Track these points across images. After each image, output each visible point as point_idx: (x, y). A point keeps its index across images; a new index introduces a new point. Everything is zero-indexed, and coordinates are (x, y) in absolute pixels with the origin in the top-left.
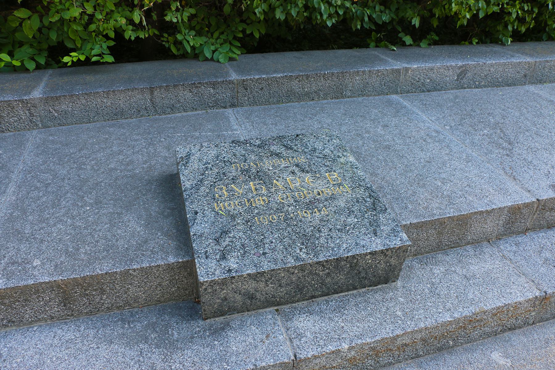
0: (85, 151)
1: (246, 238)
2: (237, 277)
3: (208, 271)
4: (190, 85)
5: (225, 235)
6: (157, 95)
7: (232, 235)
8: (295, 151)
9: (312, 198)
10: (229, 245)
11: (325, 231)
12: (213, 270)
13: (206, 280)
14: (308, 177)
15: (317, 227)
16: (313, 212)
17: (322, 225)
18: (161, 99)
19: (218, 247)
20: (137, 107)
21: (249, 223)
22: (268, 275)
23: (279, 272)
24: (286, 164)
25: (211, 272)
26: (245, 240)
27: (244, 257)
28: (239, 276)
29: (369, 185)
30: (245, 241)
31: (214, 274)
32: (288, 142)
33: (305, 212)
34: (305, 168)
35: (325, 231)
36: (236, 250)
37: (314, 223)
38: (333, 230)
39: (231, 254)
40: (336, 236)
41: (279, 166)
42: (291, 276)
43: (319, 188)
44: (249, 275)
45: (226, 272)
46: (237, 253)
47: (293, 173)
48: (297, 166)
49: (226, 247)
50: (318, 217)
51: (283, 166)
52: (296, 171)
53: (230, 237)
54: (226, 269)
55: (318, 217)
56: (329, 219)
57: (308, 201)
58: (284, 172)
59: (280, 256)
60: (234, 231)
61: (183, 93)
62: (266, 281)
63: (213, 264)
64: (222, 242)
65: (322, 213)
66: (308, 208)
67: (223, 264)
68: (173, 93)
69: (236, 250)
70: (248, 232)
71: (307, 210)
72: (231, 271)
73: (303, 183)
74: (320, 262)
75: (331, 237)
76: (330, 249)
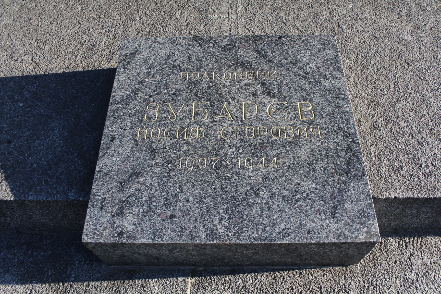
3: (96, 229)
5: (135, 179)
7: (142, 180)
8: (270, 61)
10: (133, 195)
11: (264, 196)
15: (255, 187)
16: (258, 162)
17: (263, 186)
19: (120, 195)
21: (170, 165)
24: (250, 79)
25: (99, 231)
27: (145, 216)
29: (351, 131)
30: (155, 193)
31: (101, 234)
32: (264, 46)
33: (248, 160)
34: (272, 90)
35: (264, 194)
36: (139, 204)
37: (253, 181)
38: (275, 197)
39: (132, 209)
40: (276, 207)
41: (240, 81)
43: (281, 124)
45: (116, 235)
46: (139, 208)
47: (254, 95)
48: (264, 84)
49: (129, 197)
50: (262, 172)
51: (245, 82)
52: (259, 92)
53: (139, 182)
54: (118, 230)
55: (264, 171)
56: (276, 177)
57: (258, 143)
58: (243, 91)
59: (190, 226)
60: (147, 174)
63: (105, 220)
64: (127, 188)
65: (271, 165)
66: (254, 155)
69: (139, 204)
70: (165, 179)
72: (122, 235)
73: (262, 113)
75: (269, 208)
76: (261, 227)
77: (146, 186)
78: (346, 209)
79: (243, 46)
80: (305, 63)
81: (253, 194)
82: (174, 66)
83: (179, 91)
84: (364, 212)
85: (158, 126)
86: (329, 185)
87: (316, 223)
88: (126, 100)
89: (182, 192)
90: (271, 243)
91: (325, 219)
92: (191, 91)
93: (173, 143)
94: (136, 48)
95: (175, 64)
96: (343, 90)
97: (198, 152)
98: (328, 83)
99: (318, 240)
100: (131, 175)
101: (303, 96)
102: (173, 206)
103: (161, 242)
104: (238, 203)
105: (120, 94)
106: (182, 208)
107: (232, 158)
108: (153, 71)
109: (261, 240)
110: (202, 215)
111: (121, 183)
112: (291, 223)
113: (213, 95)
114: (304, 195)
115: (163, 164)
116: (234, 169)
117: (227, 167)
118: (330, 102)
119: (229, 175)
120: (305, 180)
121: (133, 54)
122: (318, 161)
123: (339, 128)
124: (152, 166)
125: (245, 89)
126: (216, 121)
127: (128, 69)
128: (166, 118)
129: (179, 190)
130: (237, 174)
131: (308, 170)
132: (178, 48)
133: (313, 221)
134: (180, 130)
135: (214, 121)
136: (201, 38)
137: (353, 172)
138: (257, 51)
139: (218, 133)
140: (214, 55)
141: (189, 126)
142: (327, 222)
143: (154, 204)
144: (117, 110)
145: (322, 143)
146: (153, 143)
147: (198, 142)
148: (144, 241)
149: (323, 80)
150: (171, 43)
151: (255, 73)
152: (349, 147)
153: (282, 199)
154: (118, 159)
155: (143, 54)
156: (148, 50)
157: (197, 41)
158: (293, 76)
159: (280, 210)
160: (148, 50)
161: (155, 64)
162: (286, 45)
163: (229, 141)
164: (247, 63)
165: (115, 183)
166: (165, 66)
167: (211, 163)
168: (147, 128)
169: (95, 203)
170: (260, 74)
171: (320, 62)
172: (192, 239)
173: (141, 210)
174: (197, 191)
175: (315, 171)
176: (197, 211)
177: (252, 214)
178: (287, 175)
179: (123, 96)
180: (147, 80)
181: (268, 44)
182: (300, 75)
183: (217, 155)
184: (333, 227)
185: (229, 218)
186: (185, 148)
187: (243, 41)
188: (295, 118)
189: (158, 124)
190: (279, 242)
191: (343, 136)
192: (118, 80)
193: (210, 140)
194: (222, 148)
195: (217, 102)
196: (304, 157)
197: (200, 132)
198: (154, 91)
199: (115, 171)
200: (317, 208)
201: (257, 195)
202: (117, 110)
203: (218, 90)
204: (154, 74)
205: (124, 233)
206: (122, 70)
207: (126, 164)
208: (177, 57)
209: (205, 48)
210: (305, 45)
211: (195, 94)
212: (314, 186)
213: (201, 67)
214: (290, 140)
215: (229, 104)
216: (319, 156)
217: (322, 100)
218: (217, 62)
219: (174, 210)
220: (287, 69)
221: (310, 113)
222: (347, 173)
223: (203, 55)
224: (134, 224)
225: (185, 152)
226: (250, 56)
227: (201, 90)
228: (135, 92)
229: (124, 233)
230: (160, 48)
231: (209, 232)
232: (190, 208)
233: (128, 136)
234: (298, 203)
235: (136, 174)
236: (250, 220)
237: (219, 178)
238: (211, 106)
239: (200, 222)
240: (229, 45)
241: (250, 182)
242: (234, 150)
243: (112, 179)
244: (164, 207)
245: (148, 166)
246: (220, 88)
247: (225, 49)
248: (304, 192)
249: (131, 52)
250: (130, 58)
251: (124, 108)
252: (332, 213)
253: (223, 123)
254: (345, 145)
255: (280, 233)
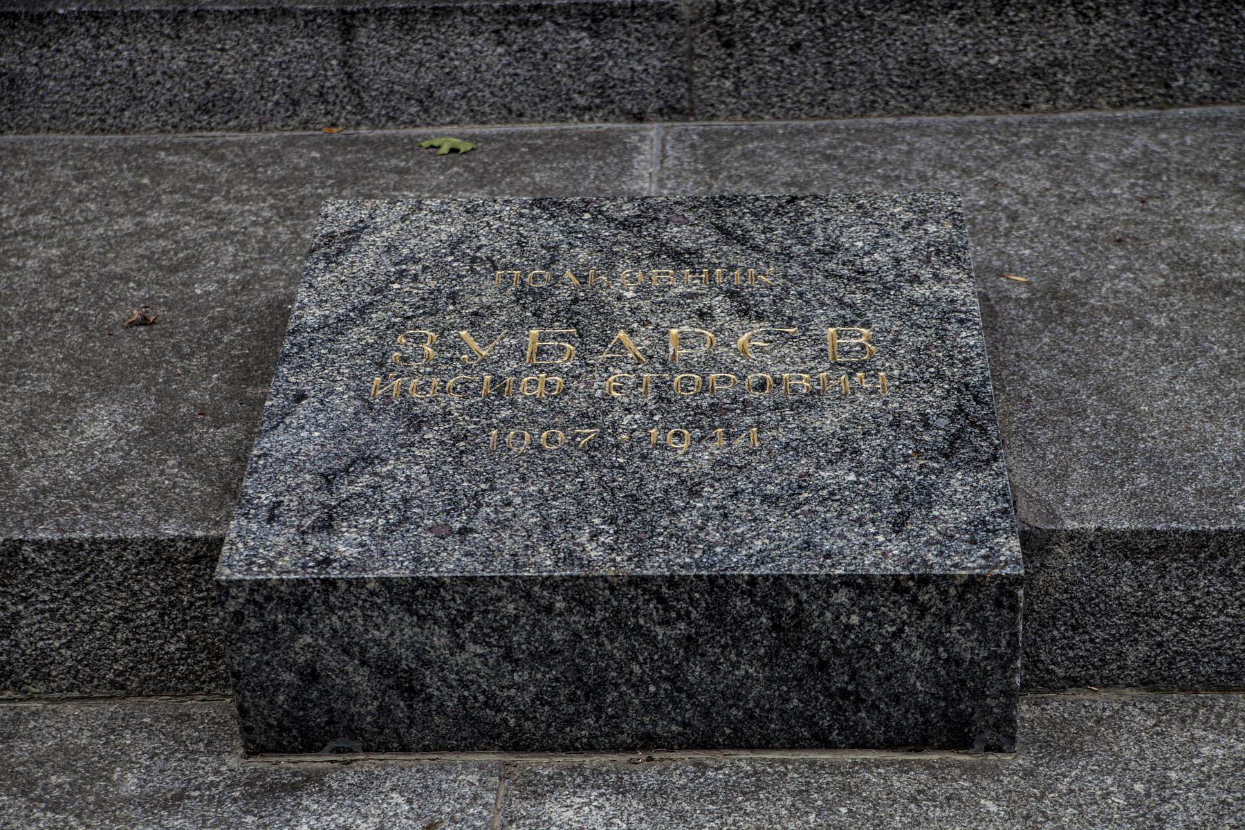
0: (42, 218)
1: (428, 483)
2: (344, 586)
4: (497, 12)
6: (367, 45)
7: (384, 469)
8: (756, 248)
9: (728, 396)
10: (360, 495)
12: (272, 554)
13: (238, 576)
14: (749, 335)
18: (383, 64)
19: (323, 497)
20: (289, 87)
21: (462, 444)
22: (454, 599)
23: (494, 591)
26: (423, 488)
28: (349, 582)
31: (271, 564)
32: (741, 218)
33: (676, 434)
34: (756, 305)
35: (714, 494)
36: (376, 511)
37: (689, 469)
42: (543, 617)
44: (385, 582)
48: (732, 294)
50: (712, 454)
51: (680, 289)
60: (398, 459)
61: (469, 45)
62: (453, 621)
65: (739, 442)
67: (314, 541)
68: (429, 41)
69: (376, 511)
71: (686, 428)
74: (645, 579)
77: (395, 479)
78: (935, 517)
79: (681, 219)
80: (861, 253)
81: (685, 493)
82: (474, 260)
83: (489, 307)
84: (984, 523)
85: (430, 373)
86: (893, 476)
87: (849, 540)
88: (336, 328)
89: (493, 489)
90: (724, 576)
91: (875, 534)
92: (524, 308)
93: (472, 405)
94: (361, 221)
95: (479, 254)
96: (964, 304)
97: (540, 420)
98: (919, 292)
99: (852, 568)
100: (353, 462)
101: (844, 317)
102: (467, 514)
103: (435, 575)
104: (642, 508)
105: (318, 313)
106: (493, 516)
107: (634, 430)
108: (414, 269)
109: (698, 568)
110: (546, 527)
111: (325, 476)
112: (781, 539)
113: (585, 316)
114: (825, 493)
115: (442, 443)
116: (637, 450)
117: (617, 446)
118: (920, 327)
119: (621, 460)
120: (829, 468)
121: (355, 233)
122: (870, 435)
123: (940, 376)
124: (412, 444)
125: (679, 304)
126: (593, 365)
127: (340, 264)
128: (451, 359)
129: (483, 486)
130: (644, 457)
131: (838, 450)
132: (488, 223)
133: (842, 536)
134: (493, 381)
135: (588, 365)
136: (555, 203)
137: (965, 453)
138: (721, 229)
139: (596, 386)
140: (595, 239)
141: (516, 373)
142: (881, 538)
143: (416, 510)
144: (311, 345)
145: (885, 403)
146: (415, 404)
147: (540, 403)
148: (388, 572)
149: (907, 286)
150: (467, 211)
151: (711, 272)
152: (960, 409)
153: (762, 502)
154: (317, 434)
155: (384, 233)
156: (397, 227)
157: (544, 209)
158: (820, 278)
159: (755, 520)
160: (397, 227)
161: (421, 255)
162: (809, 215)
163: (626, 400)
164: (690, 254)
165: (308, 477)
166: (450, 259)
167: (573, 439)
168: (397, 377)
169: (252, 511)
170: (725, 276)
171: (905, 249)
172: (516, 565)
173: (381, 522)
174: (533, 488)
175: (857, 452)
176: (534, 520)
177: (680, 525)
178: (780, 458)
179: (327, 317)
180: (396, 286)
181: (754, 214)
182: (841, 277)
183: (590, 426)
184: (896, 548)
185: (616, 532)
186: (505, 413)
187: (681, 208)
188: (815, 358)
189: (428, 369)
190: (745, 572)
191: (948, 391)
192: (311, 286)
193: (574, 398)
194: (605, 413)
195: (597, 329)
196: (828, 429)
197: (548, 384)
198: (419, 307)
199: (307, 455)
200: (855, 515)
201: (694, 492)
202: (311, 345)
203: (603, 307)
204: (416, 275)
205: (335, 561)
206: (322, 265)
207: (340, 443)
208: (484, 241)
209: (567, 223)
210: (865, 214)
211: (534, 314)
212: (852, 477)
213: (553, 261)
214: (795, 398)
215: (631, 332)
216: (874, 426)
217: (899, 323)
218: (601, 251)
219: (470, 520)
220: (804, 265)
221: (858, 348)
222: (946, 456)
223: (561, 237)
224: (362, 545)
225: (504, 421)
226: (698, 239)
227: (552, 306)
228: (363, 310)
229: (335, 561)
230: (436, 223)
231: (562, 555)
232: (515, 516)
233: (343, 393)
234: (806, 508)
235: (369, 461)
236: (672, 535)
237: (594, 464)
238: (581, 336)
239: (538, 540)
240: (639, 216)
241: (677, 470)
242: (637, 417)
243: (298, 469)
244: (444, 516)
245: (401, 446)
246: (609, 303)
247: (625, 224)
248: (823, 488)
249: (347, 229)
250: (345, 241)
251: (330, 340)
252: (895, 524)
253: (611, 369)
254: (950, 405)
255: (749, 557)
